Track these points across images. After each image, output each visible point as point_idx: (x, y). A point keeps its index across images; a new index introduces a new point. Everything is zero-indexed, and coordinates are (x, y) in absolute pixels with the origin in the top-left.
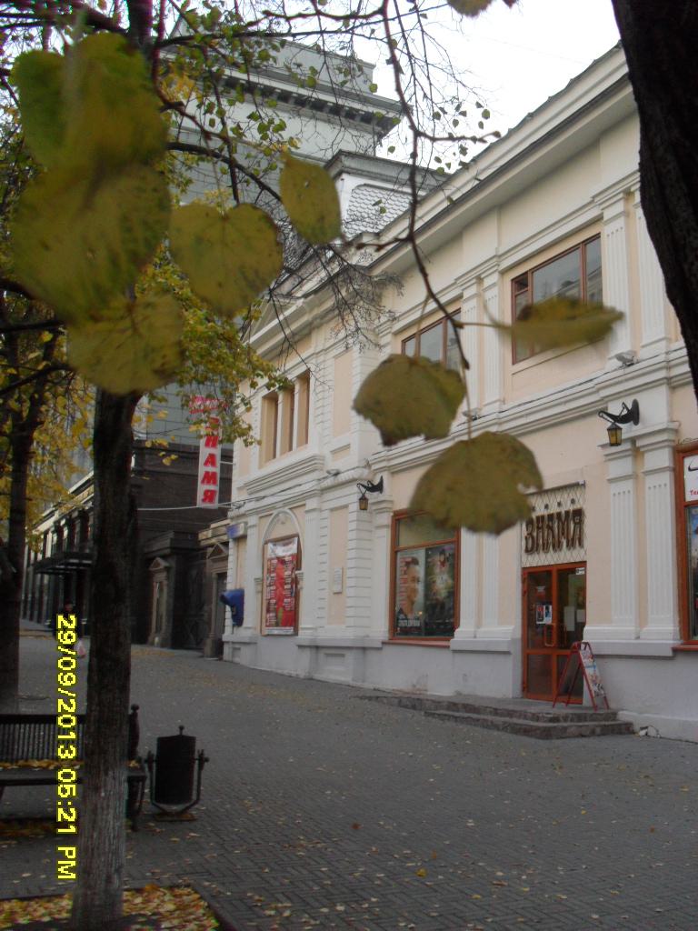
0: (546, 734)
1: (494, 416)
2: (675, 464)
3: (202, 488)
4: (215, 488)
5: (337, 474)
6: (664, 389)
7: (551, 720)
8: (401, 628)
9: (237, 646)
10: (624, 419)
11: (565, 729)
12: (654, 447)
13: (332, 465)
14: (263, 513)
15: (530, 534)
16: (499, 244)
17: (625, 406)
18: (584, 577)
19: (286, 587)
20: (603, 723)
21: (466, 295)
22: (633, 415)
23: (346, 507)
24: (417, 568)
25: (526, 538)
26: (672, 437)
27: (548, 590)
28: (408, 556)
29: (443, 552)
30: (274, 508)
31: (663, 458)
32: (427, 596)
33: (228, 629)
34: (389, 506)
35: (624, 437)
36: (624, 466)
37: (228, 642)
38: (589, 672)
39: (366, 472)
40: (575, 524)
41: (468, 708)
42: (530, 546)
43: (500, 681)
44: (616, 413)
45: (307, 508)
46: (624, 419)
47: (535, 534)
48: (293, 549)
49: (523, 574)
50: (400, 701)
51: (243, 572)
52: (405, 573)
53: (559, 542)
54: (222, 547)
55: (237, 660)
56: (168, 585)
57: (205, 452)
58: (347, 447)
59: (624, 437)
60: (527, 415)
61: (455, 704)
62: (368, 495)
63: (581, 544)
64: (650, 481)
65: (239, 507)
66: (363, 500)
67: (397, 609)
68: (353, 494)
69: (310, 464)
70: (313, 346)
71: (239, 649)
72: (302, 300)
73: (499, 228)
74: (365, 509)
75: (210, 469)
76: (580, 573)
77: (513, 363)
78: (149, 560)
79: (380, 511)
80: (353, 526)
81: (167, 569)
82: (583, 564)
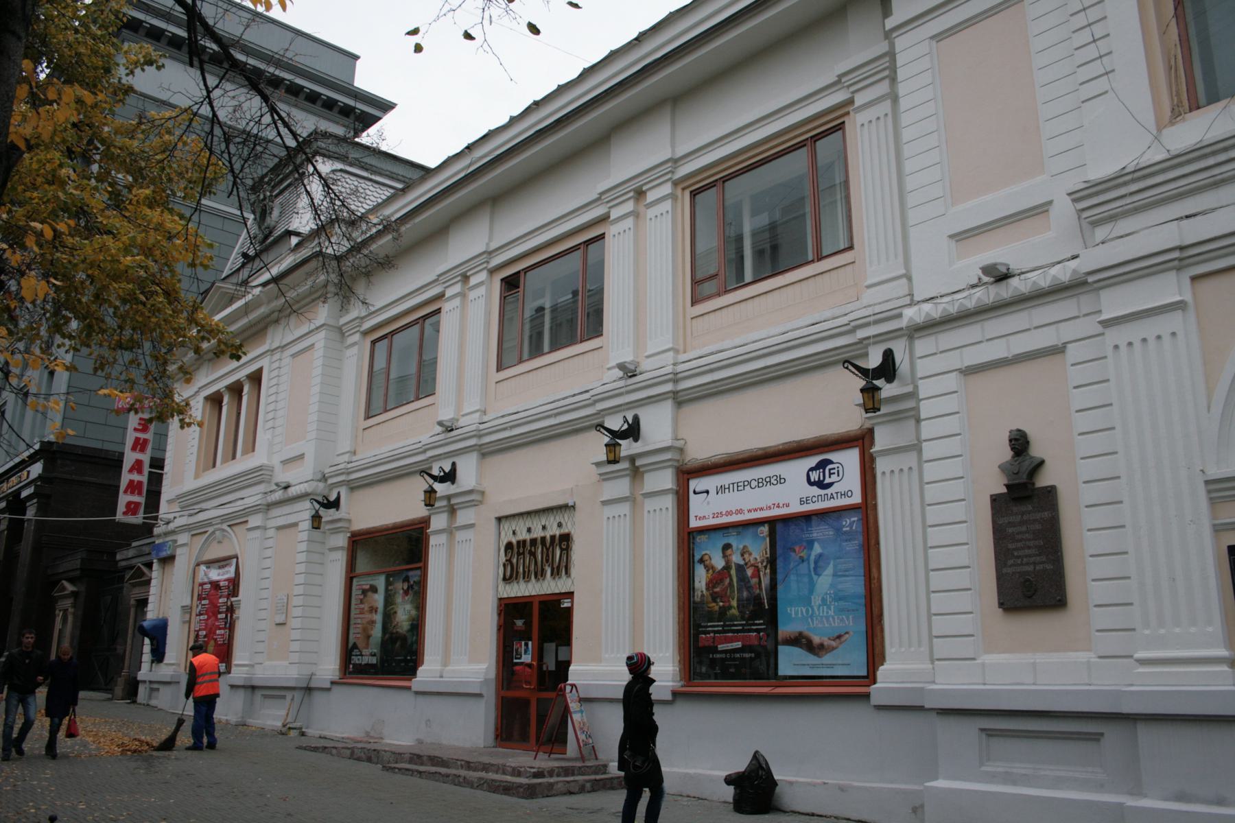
0: (531, 792)
1: (473, 427)
2: (678, 485)
3: (123, 499)
4: (141, 499)
5: (286, 488)
6: (668, 406)
7: (536, 775)
8: (354, 665)
9: (155, 686)
10: (623, 435)
11: (551, 785)
12: (657, 466)
13: (282, 476)
14: (196, 530)
15: (509, 561)
16: (490, 239)
17: (626, 421)
18: (569, 611)
19: (220, 616)
20: (593, 777)
21: (448, 293)
22: (633, 431)
23: (295, 525)
24: (376, 596)
25: (504, 565)
26: (677, 457)
27: (528, 624)
28: (365, 583)
29: (406, 579)
30: (211, 525)
31: (665, 480)
32: (385, 628)
33: (145, 666)
34: (346, 525)
35: (622, 454)
36: (622, 487)
37: (144, 682)
38: (576, 717)
39: (321, 485)
40: (562, 550)
41: (434, 761)
42: (508, 574)
43: (470, 730)
44: (616, 428)
45: (250, 525)
46: (623, 435)
47: (514, 561)
48: (230, 572)
49: (500, 605)
50: (353, 753)
51: (169, 597)
52: (362, 602)
53: (543, 570)
54: (145, 569)
55: (153, 702)
56: (74, 614)
57: (130, 457)
58: (301, 456)
59: (622, 454)
60: (512, 427)
61: (419, 756)
62: (322, 512)
64: (649, 505)
65: (168, 523)
66: (316, 520)
67: (350, 645)
68: (304, 512)
69: (258, 476)
70: (268, 342)
71: (158, 690)
72: (259, 289)
73: (491, 229)
74: (318, 528)
75: (136, 477)
76: (566, 605)
77: (498, 371)
78: (54, 583)
79: (336, 531)
80: (303, 547)
81: (74, 595)
82: (570, 595)
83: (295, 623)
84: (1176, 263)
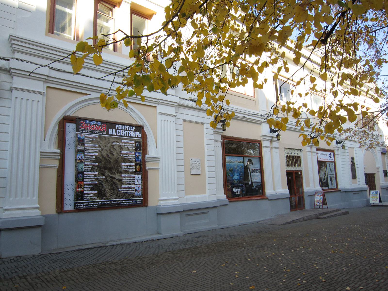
50: (304, 219)
63: (301, 166)
84: (44, 80)
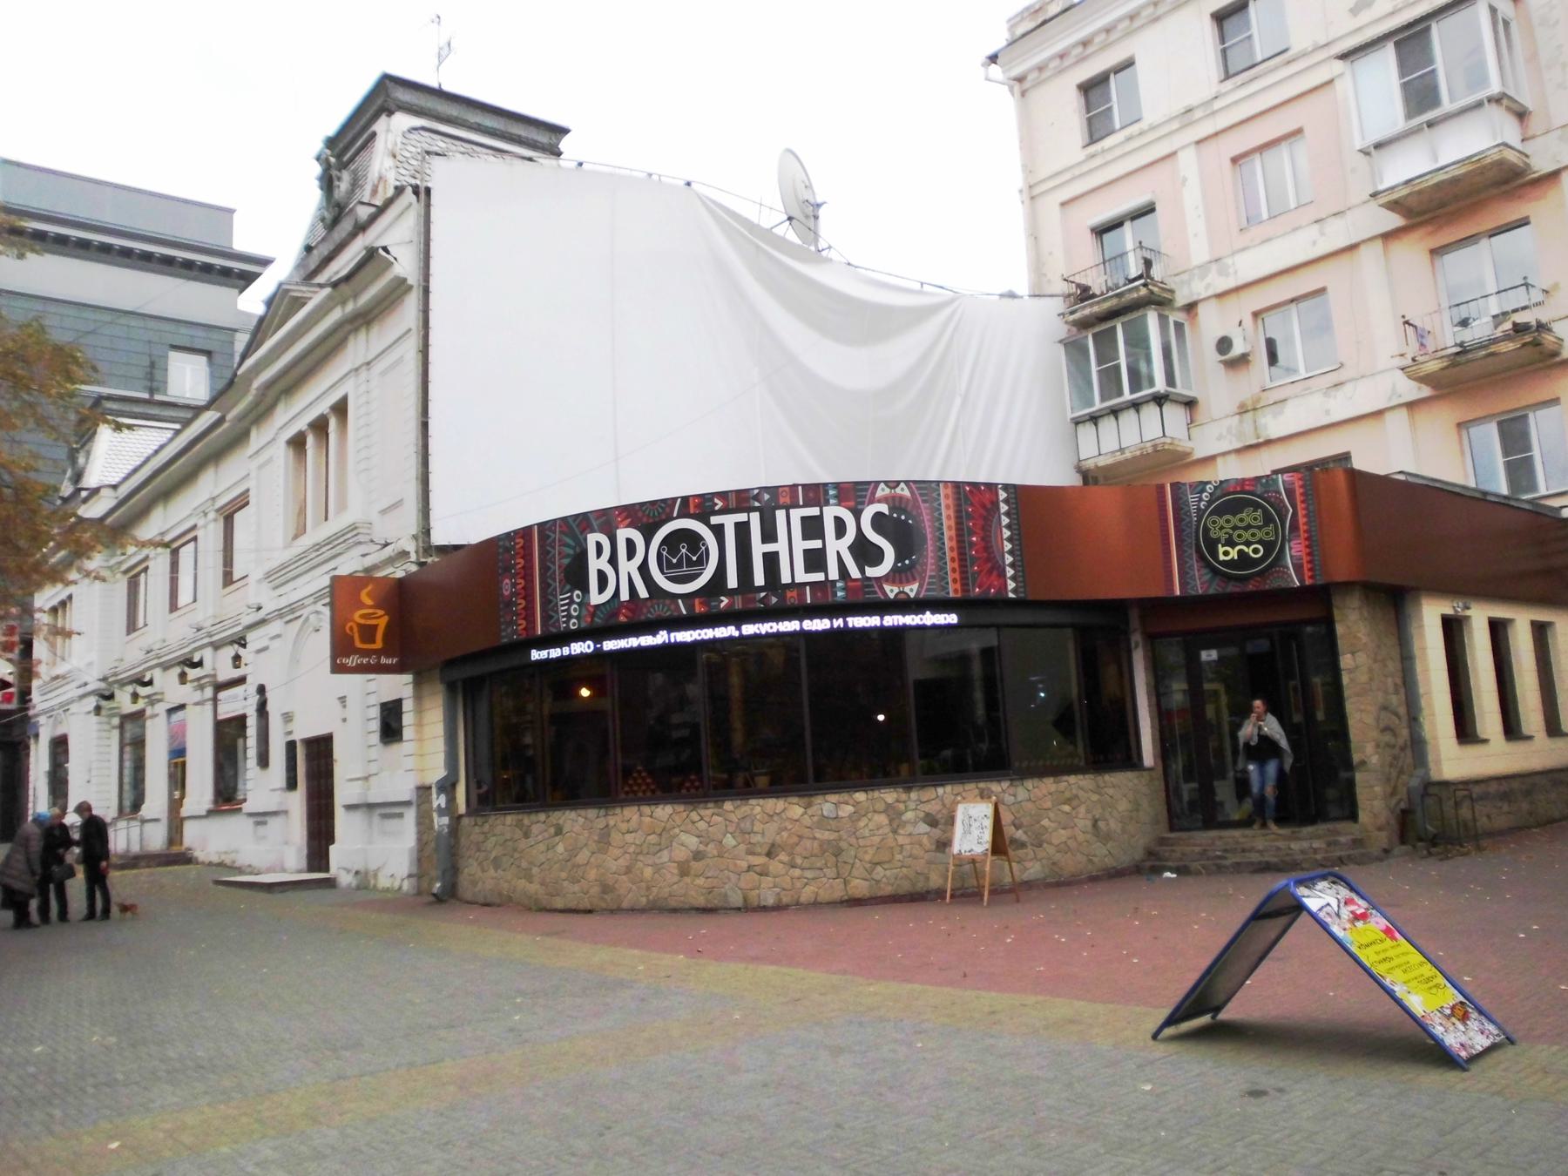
31: (209, 692)
36: (197, 696)
62: (104, 703)
83: (94, 780)
